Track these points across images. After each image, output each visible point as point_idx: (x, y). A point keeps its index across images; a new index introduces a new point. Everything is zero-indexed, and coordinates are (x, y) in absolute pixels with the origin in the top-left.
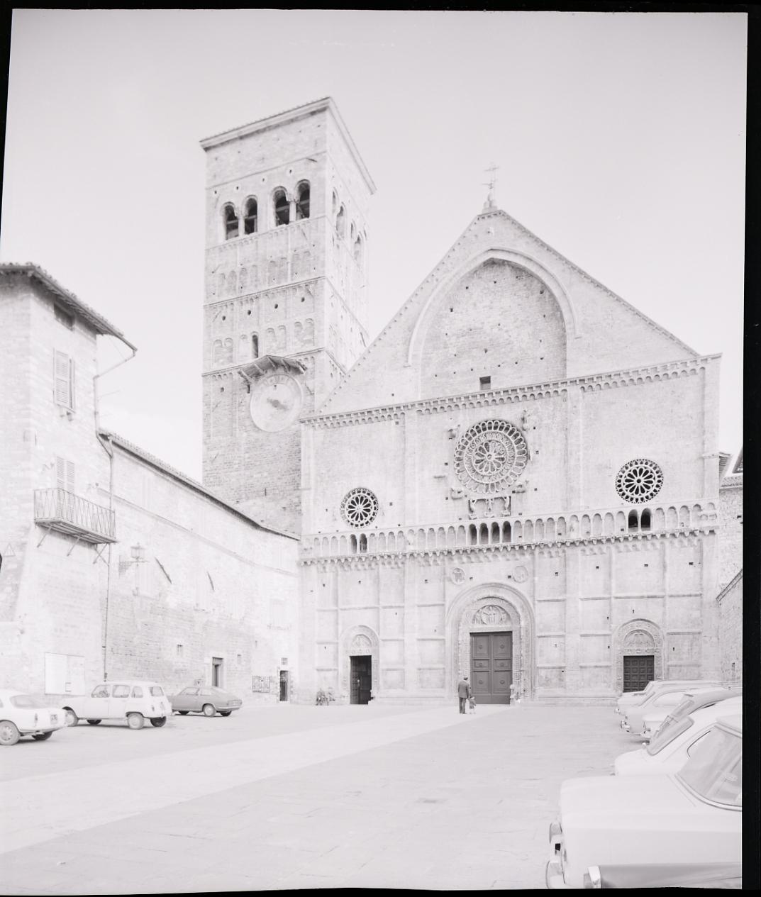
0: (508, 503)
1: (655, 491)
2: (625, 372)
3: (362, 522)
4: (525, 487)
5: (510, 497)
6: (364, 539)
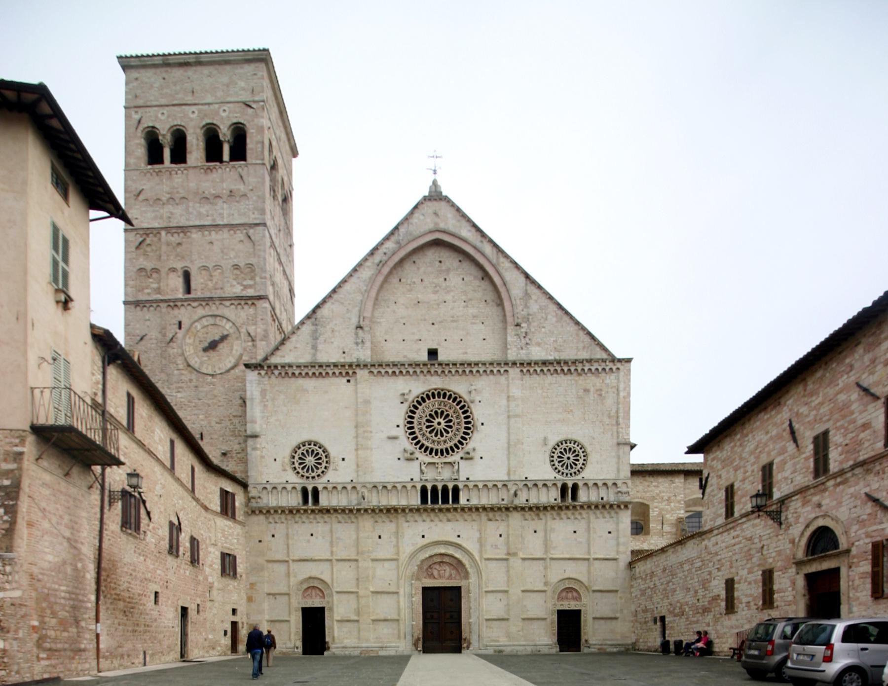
0: (456, 467)
1: (581, 468)
3: (313, 474)
4: (472, 454)
6: (316, 491)
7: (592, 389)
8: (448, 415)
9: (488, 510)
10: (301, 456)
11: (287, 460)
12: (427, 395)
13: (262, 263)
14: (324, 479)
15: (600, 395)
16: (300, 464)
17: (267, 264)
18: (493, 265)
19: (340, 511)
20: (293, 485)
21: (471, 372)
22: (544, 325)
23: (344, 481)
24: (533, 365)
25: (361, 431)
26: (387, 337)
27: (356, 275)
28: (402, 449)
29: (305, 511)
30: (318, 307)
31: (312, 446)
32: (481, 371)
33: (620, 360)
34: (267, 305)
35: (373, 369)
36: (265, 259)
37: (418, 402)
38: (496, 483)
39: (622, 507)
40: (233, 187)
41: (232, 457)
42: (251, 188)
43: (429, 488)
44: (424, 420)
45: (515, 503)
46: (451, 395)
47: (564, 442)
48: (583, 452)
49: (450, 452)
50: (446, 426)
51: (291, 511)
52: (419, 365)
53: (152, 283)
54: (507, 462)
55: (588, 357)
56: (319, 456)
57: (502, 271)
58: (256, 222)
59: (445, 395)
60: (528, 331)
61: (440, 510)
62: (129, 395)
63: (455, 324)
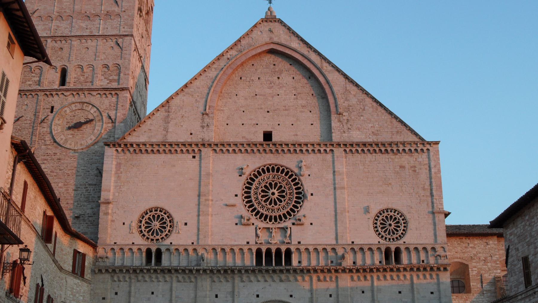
2: (383, 143)
3: (157, 237)
4: (303, 220)
5: (290, 228)
6: (159, 253)
7: (407, 166)
8: (281, 187)
9: (319, 271)
10: (147, 220)
11: (135, 224)
12: (263, 170)
13: (126, 63)
14: (167, 242)
15: (415, 171)
16: (146, 228)
17: (131, 65)
18: (318, 69)
19: (180, 271)
20: (138, 247)
21: (301, 151)
22: (363, 114)
23: (185, 244)
24: (354, 146)
25: (202, 199)
26: (228, 122)
27: (204, 75)
28: (240, 214)
29: (148, 270)
30: (171, 98)
31: (158, 212)
32: (310, 150)
33: (429, 143)
34: (128, 95)
35: (215, 148)
36: (129, 61)
37: (254, 175)
38: (325, 247)
39: (442, 269)
40: (108, 9)
41: (84, 220)
42: (123, 10)
43: (264, 251)
44: (260, 190)
45: (343, 265)
46: (283, 170)
47: (385, 211)
48: (403, 220)
49: (283, 218)
50: (278, 196)
51: (135, 271)
52: (256, 145)
53: (34, 77)
54: (334, 228)
55: (401, 140)
56: (164, 221)
57: (326, 74)
58: (124, 34)
59: (278, 170)
60: (349, 118)
61: (274, 271)
62: (26, 184)
63: (286, 112)
